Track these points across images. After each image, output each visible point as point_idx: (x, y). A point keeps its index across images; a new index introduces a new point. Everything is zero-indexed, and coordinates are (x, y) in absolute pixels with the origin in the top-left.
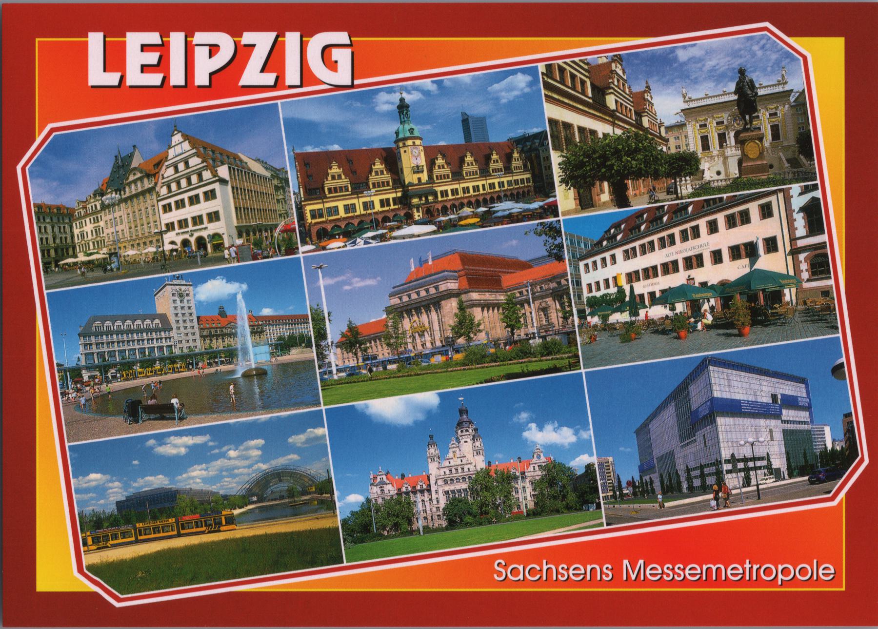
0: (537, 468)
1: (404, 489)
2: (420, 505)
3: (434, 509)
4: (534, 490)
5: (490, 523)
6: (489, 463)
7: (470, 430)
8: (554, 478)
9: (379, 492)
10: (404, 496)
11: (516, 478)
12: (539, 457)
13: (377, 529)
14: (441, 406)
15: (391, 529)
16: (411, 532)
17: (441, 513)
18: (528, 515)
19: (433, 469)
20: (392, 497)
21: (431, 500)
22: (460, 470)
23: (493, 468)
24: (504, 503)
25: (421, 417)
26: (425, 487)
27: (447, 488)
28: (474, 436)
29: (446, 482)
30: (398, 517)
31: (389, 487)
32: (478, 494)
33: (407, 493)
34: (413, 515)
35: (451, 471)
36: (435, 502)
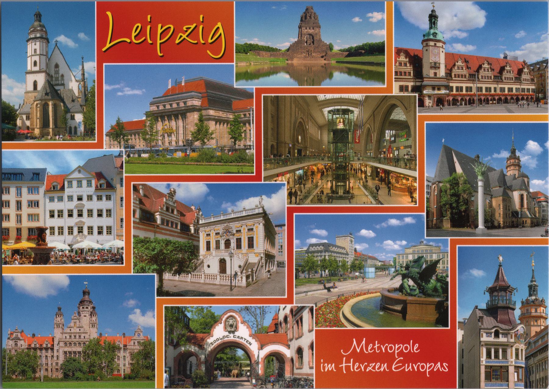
0: (136, 343)
2: (44, 360)
3: (54, 364)
4: (132, 360)
5: (95, 379)
6: (101, 334)
7: (89, 308)
8: (149, 353)
9: (13, 345)
10: (32, 350)
11: (119, 349)
12: (139, 335)
13: (8, 373)
14: (70, 285)
16: (34, 379)
17: (59, 367)
18: (125, 378)
20: (23, 350)
21: (53, 356)
22: (77, 337)
23: (103, 339)
24: (108, 366)
25: (53, 292)
26: (49, 346)
28: (91, 312)
30: (25, 366)
31: (22, 342)
32: (88, 357)
33: (35, 349)
35: (70, 336)
36: (55, 358)
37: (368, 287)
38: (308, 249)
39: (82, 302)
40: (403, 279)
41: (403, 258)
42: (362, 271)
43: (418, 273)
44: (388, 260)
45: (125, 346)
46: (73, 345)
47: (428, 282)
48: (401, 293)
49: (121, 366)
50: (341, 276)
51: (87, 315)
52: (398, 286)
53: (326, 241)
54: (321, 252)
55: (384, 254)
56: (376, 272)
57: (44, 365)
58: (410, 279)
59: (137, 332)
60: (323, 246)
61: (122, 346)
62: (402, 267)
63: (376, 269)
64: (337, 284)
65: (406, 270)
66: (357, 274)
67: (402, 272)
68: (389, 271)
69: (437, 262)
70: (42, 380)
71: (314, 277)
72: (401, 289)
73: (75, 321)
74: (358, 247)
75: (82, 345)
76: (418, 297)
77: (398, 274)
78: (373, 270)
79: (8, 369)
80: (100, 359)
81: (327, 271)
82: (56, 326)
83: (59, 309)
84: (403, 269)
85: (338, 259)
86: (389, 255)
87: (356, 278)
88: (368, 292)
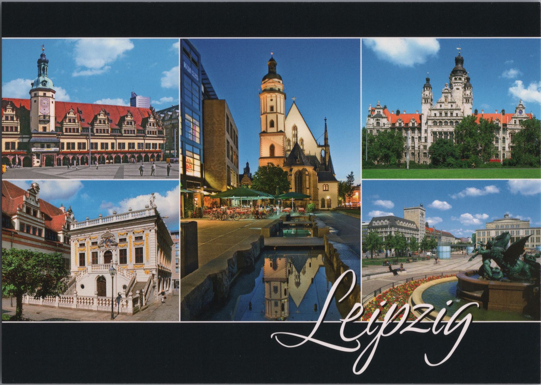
0: (518, 123)
1: (397, 125)
2: (410, 141)
3: (422, 147)
4: (513, 142)
5: (470, 166)
7: (463, 79)
9: (375, 124)
10: (397, 131)
11: (498, 129)
12: (521, 112)
13: (369, 158)
15: (381, 159)
16: (399, 165)
19: (425, 109)
21: (420, 138)
22: (449, 114)
23: (478, 116)
24: (484, 150)
27: (435, 129)
28: (465, 85)
29: (435, 123)
30: (389, 149)
33: (400, 129)
34: (403, 149)
35: (441, 114)
36: (423, 140)
37: (442, 270)
38: (371, 223)
39: (454, 72)
40: (484, 260)
41: (484, 235)
42: (434, 250)
43: (502, 253)
44: (466, 237)
45: (505, 125)
46: (443, 124)
47: (514, 263)
48: (481, 277)
49: (500, 149)
50: (410, 256)
51: (460, 88)
52: (478, 269)
53: (391, 214)
54: (386, 227)
55: (461, 230)
56: (451, 251)
57: (411, 149)
58: (492, 260)
59: (520, 108)
60: (389, 220)
61: (500, 125)
62: (482, 245)
63: (452, 247)
64: (405, 265)
65: (487, 249)
66: (429, 254)
67: (482, 252)
68: (467, 250)
69: (526, 239)
70: (408, 167)
71: (378, 257)
72: (482, 271)
73: (446, 95)
74: (430, 222)
75: (454, 124)
76: (502, 281)
77: (478, 254)
78: (448, 248)
79: (368, 153)
80: (476, 141)
81: (393, 250)
82: (424, 101)
83: (428, 80)
84: (485, 248)
85: (407, 236)
86: (468, 231)
87: (428, 258)
88: (442, 275)
